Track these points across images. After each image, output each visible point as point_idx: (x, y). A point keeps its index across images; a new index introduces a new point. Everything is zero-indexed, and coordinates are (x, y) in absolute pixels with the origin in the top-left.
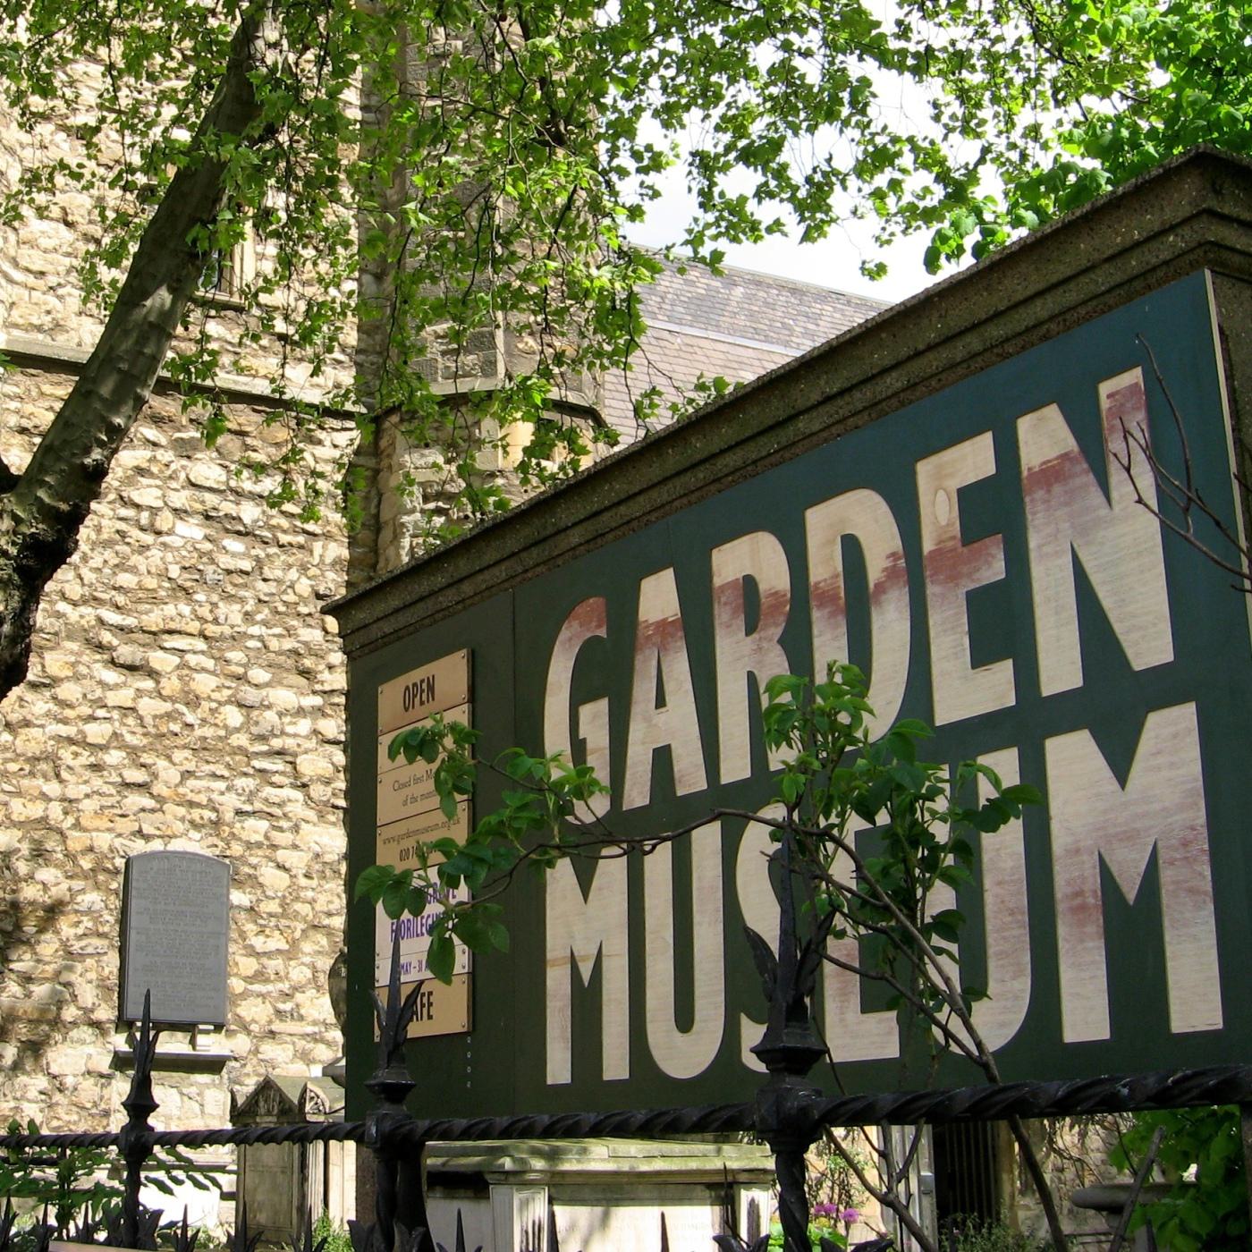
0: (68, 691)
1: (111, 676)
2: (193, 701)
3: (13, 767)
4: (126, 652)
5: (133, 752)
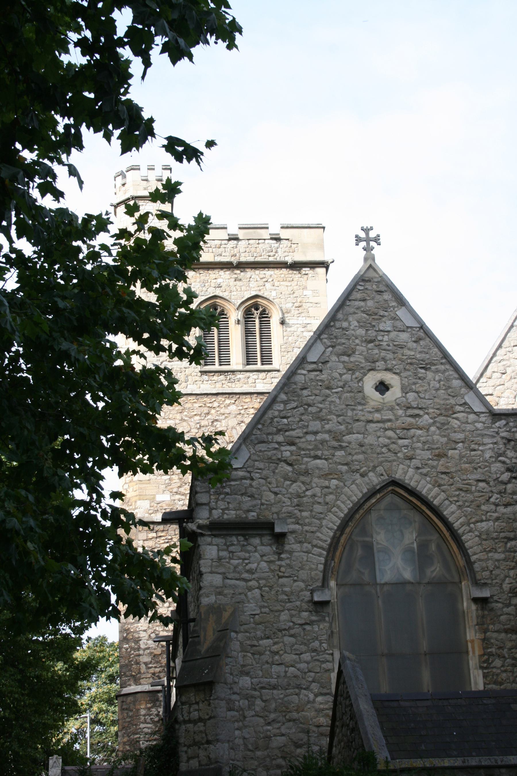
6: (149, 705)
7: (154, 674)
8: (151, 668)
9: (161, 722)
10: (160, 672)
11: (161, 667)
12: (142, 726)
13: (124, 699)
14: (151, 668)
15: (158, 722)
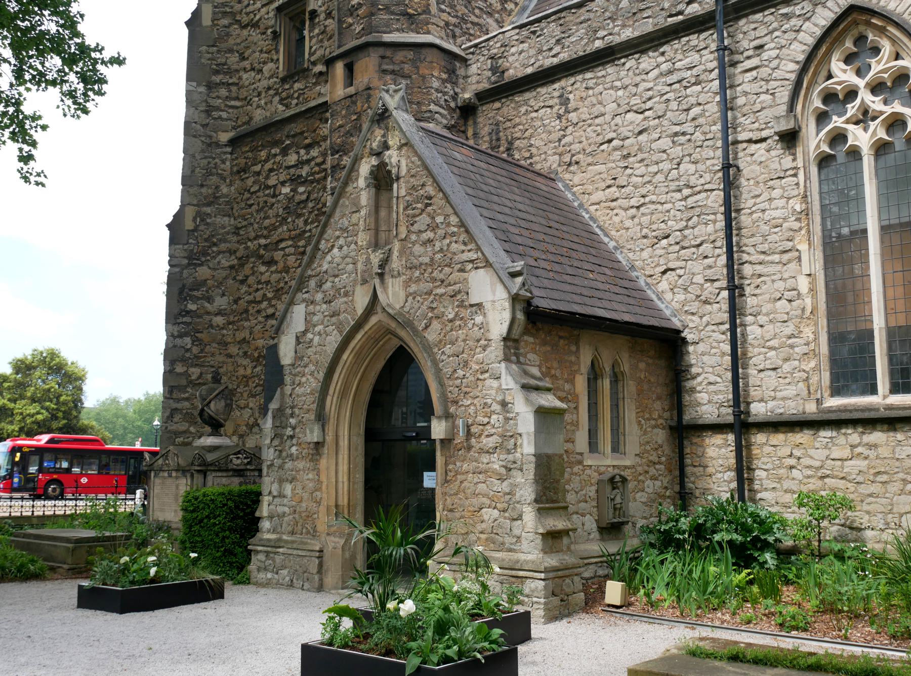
0: (251, 280)
1: (263, 269)
2: (286, 270)
3: (236, 318)
4: (267, 256)
5: (269, 300)
6: (444, 76)
7: (447, 24)
8: (444, 11)
9: (458, 110)
10: (454, 25)
11: (457, 17)
12: (433, 107)
13: (388, 53)
14: (444, 11)
15: (454, 110)
